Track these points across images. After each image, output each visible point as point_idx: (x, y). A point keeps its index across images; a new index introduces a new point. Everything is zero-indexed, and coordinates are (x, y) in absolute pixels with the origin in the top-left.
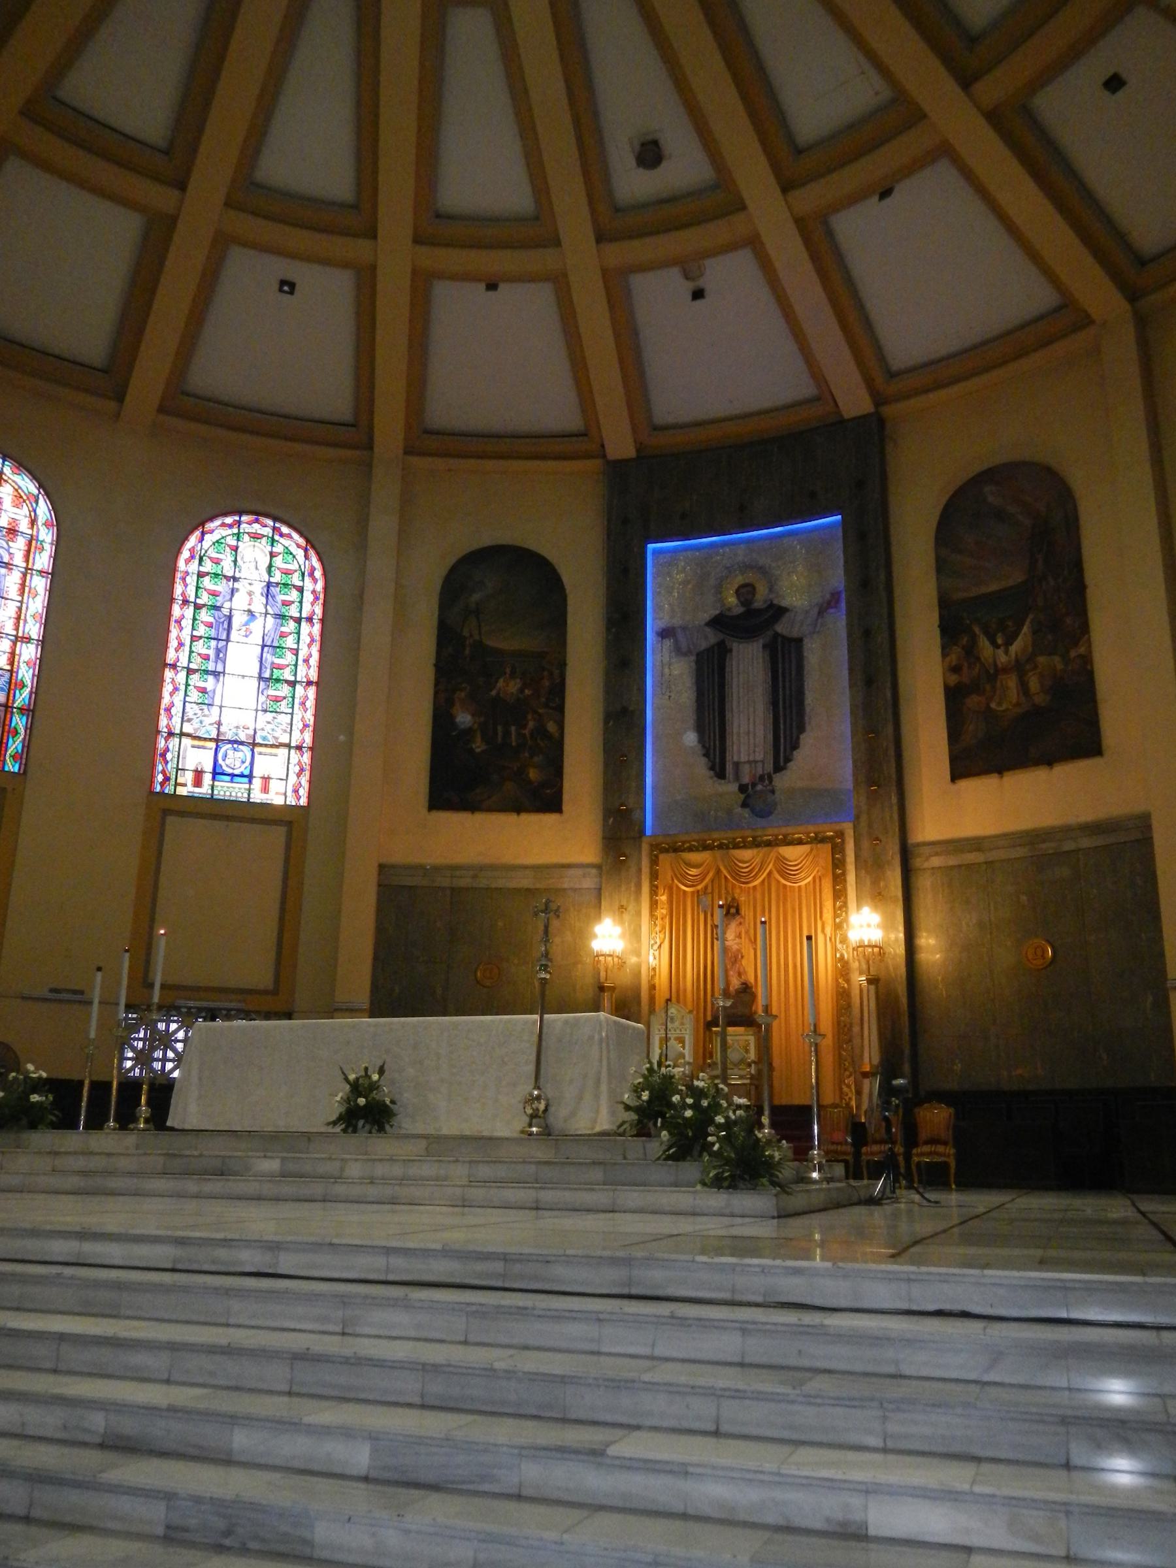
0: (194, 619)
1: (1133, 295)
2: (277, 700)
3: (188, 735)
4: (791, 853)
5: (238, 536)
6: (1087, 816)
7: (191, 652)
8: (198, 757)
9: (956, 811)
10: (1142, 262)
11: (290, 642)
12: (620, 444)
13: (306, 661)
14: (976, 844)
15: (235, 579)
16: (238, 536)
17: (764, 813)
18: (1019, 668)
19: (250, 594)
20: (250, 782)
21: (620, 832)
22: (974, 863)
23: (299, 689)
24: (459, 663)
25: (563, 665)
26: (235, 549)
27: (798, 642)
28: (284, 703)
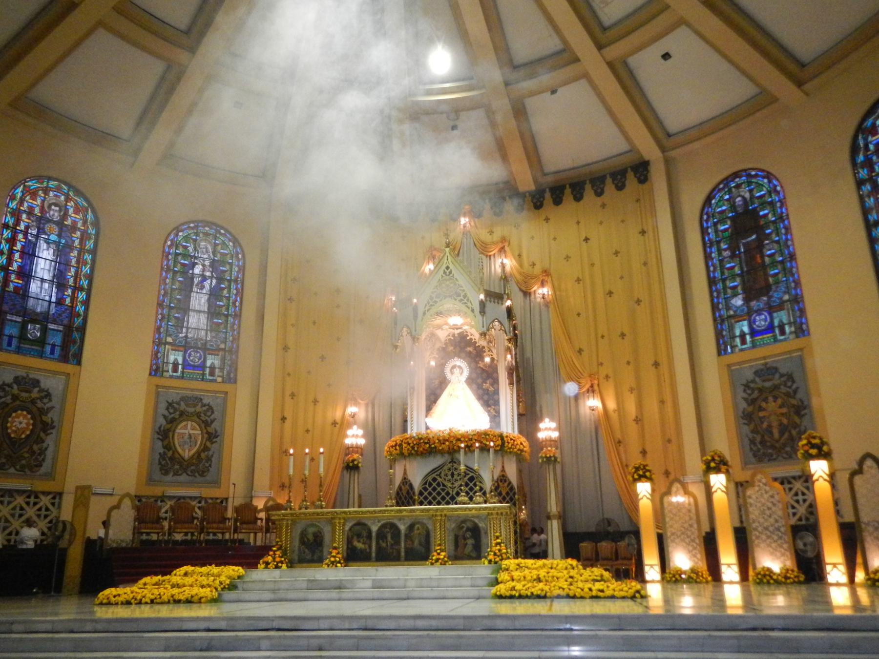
0: (173, 279)
1: (663, 149)
2: (218, 324)
3: (169, 343)
5: (197, 234)
7: (171, 297)
11: (225, 292)
13: (234, 303)
15: (196, 258)
16: (197, 234)
19: (204, 265)
20: (204, 370)
23: (230, 319)
26: (195, 240)
28: (222, 326)
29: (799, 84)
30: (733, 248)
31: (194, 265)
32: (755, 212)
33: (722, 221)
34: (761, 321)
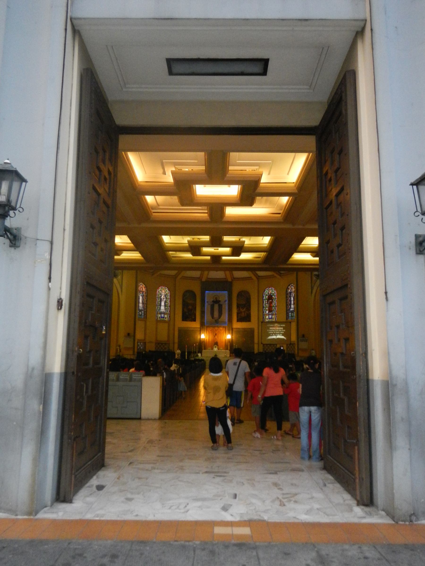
1: (258, 279)
4: (221, 328)
6: (250, 327)
8: (159, 316)
9: (237, 325)
10: (259, 276)
12: (204, 280)
14: (239, 329)
17: (217, 323)
18: (244, 312)
21: (202, 325)
22: (238, 331)
24: (185, 304)
25: (196, 305)
27: (221, 305)
29: (280, 276)
30: (268, 301)
31: (161, 296)
32: (272, 296)
33: (267, 296)
34: (270, 316)
